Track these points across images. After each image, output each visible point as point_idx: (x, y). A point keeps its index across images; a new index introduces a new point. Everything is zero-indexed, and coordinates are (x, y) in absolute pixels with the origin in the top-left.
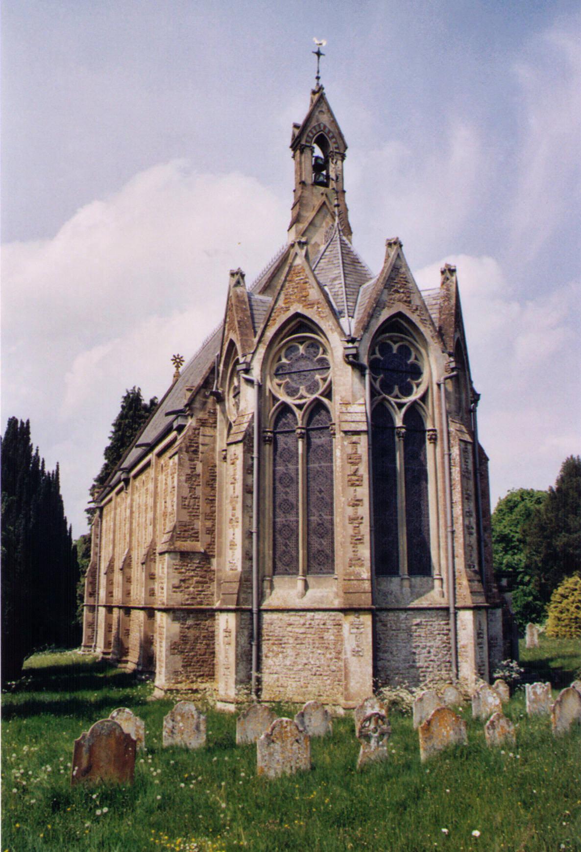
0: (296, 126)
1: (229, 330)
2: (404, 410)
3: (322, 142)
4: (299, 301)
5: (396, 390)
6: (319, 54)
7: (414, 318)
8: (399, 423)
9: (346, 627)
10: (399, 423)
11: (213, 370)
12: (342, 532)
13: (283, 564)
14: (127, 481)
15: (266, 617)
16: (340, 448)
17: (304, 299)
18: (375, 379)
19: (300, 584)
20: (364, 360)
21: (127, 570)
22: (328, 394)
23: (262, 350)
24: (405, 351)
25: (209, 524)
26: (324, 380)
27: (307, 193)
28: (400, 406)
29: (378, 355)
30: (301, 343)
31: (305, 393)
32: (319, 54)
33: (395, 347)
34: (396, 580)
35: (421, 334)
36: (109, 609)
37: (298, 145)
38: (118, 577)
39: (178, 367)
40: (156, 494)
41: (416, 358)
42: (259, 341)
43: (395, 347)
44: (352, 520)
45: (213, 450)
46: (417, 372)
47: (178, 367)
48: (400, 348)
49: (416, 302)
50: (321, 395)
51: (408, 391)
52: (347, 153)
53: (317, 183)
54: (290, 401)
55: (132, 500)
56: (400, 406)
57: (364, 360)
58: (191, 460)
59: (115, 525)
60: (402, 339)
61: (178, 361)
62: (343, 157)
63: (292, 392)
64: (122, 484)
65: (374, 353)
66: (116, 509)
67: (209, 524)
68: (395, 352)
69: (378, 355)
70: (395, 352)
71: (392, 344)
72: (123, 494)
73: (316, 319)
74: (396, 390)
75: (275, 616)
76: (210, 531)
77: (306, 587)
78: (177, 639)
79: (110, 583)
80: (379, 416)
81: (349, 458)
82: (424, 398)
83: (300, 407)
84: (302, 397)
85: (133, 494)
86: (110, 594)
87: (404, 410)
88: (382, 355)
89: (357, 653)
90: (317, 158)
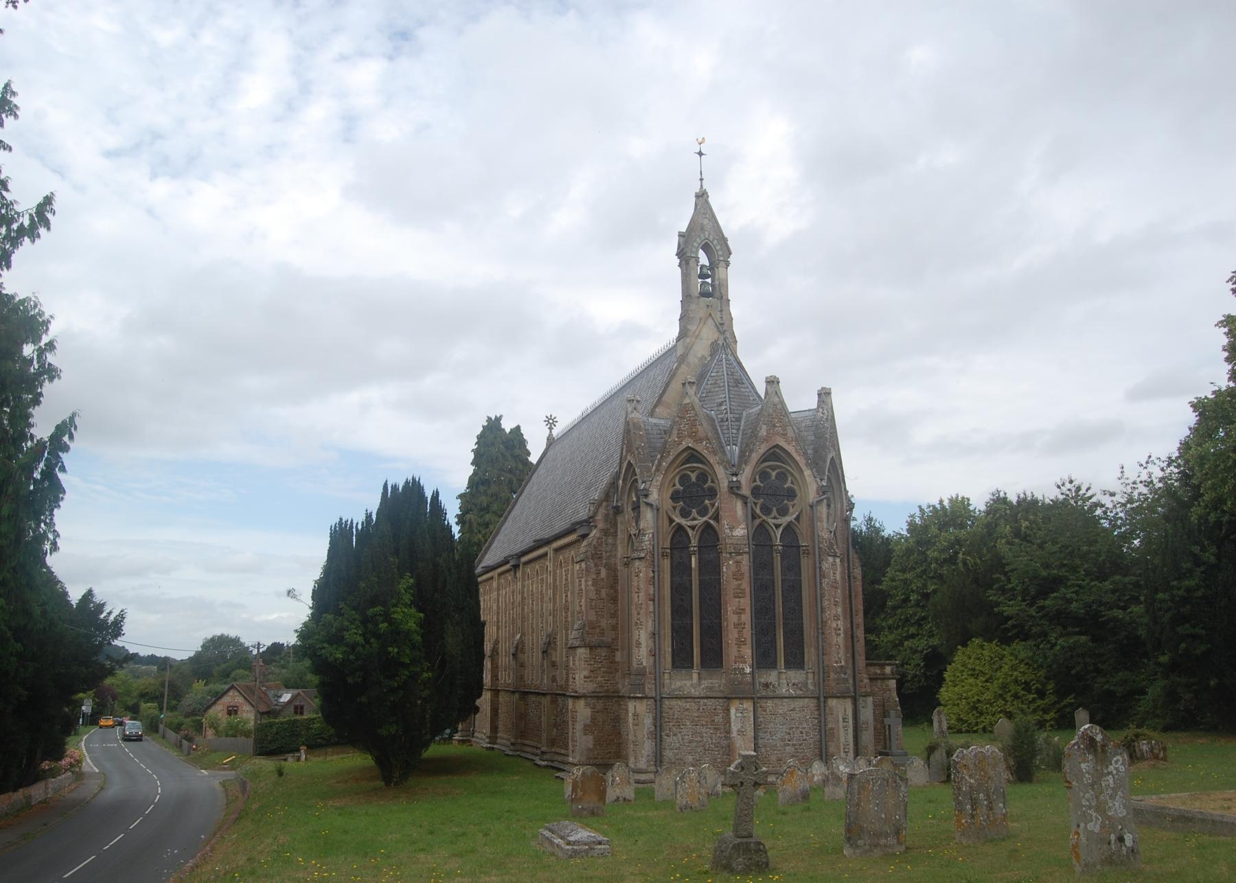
0: (681, 235)
1: (627, 452)
2: (781, 529)
3: (707, 248)
4: (690, 436)
5: (774, 513)
6: (700, 154)
7: (790, 449)
9: (733, 711)
11: (613, 484)
12: (731, 635)
13: (682, 660)
14: (516, 567)
15: (666, 702)
16: (728, 568)
17: (693, 435)
18: (755, 504)
19: (695, 676)
20: (745, 491)
21: (520, 655)
22: (716, 517)
23: (660, 478)
24: (782, 476)
25: (613, 621)
26: (713, 505)
27: (693, 307)
28: (777, 526)
29: (758, 483)
32: (700, 154)
34: (774, 673)
36: (496, 692)
37: (684, 256)
38: (504, 660)
39: (551, 429)
40: (555, 587)
42: (657, 470)
43: (774, 474)
44: (736, 625)
45: (615, 556)
46: (791, 494)
47: (551, 429)
48: (778, 476)
49: (790, 433)
51: (783, 512)
52: (731, 259)
53: (704, 294)
54: (683, 522)
55: (523, 586)
56: (777, 526)
57: (745, 491)
58: (596, 565)
59: (498, 607)
60: (779, 467)
61: (551, 422)
62: (728, 264)
63: (685, 514)
64: (507, 567)
66: (498, 590)
67: (613, 621)
69: (758, 483)
72: (509, 577)
73: (705, 453)
74: (774, 513)
75: (674, 702)
76: (614, 628)
77: (700, 678)
78: (588, 722)
79: (495, 668)
80: (760, 534)
81: (736, 574)
82: (797, 519)
83: (693, 528)
84: (694, 519)
85: (524, 580)
86: (495, 677)
87: (781, 529)
89: (740, 732)
90: (702, 266)
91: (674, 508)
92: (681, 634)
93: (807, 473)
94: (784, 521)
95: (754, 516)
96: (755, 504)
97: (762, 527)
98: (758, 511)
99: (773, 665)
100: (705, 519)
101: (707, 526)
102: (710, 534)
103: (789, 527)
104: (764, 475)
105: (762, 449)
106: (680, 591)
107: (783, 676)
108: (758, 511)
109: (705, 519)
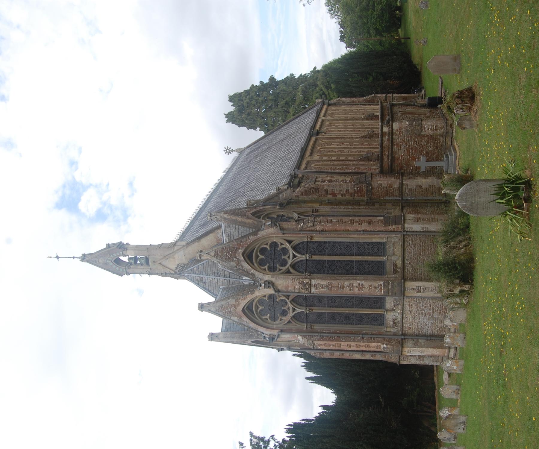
8: (303, 257)
10: (303, 257)
13: (379, 320)
24: (263, 251)
29: (266, 267)
30: (258, 308)
31: (287, 307)
33: (261, 257)
35: (254, 241)
41: (267, 244)
43: (261, 257)
46: (274, 245)
48: (262, 254)
50: (288, 299)
56: (294, 256)
60: (257, 252)
63: (284, 313)
65: (265, 269)
68: (263, 257)
69: (266, 267)
70: (263, 257)
71: (259, 258)
82: (290, 242)
83: (294, 310)
84: (289, 308)
88: (266, 265)
91: (281, 320)
92: (361, 319)
93: (261, 234)
94: (291, 251)
95: (288, 272)
96: (280, 270)
97: (293, 266)
98: (284, 269)
99: (381, 264)
100: (288, 301)
101: (293, 301)
102: (296, 301)
103: (294, 248)
104: (261, 263)
105: (245, 265)
106: (333, 319)
107: (389, 258)
108: (284, 269)
109: (288, 301)
